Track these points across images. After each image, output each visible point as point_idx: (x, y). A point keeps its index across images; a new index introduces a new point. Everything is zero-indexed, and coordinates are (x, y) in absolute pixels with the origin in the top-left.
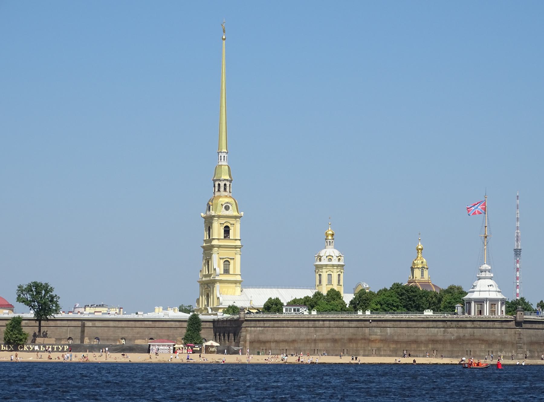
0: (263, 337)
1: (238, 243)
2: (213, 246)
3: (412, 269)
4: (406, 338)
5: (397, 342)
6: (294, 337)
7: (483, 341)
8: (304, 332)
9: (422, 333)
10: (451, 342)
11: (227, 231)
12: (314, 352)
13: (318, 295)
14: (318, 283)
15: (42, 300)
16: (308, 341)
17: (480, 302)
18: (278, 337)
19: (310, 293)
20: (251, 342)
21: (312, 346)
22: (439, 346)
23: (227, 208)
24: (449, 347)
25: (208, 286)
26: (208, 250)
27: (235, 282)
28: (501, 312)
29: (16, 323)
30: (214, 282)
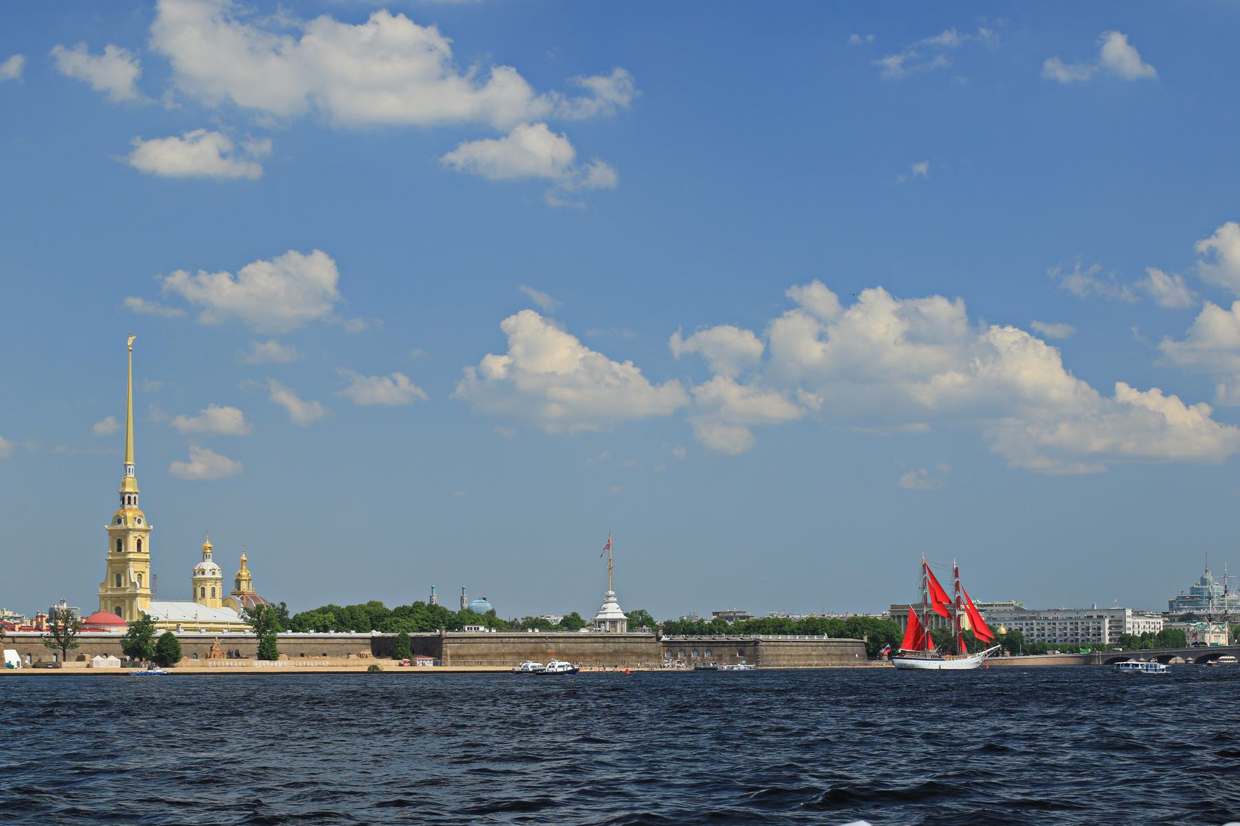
0: (460, 652)
1: (148, 557)
2: (130, 560)
3: (238, 582)
4: (575, 652)
5: (568, 655)
6: (486, 651)
7: (633, 653)
14: (199, 595)
17: (614, 622)
18: (472, 652)
20: (452, 656)
22: (601, 658)
23: (139, 522)
24: (608, 658)
27: (146, 596)
30: (137, 595)
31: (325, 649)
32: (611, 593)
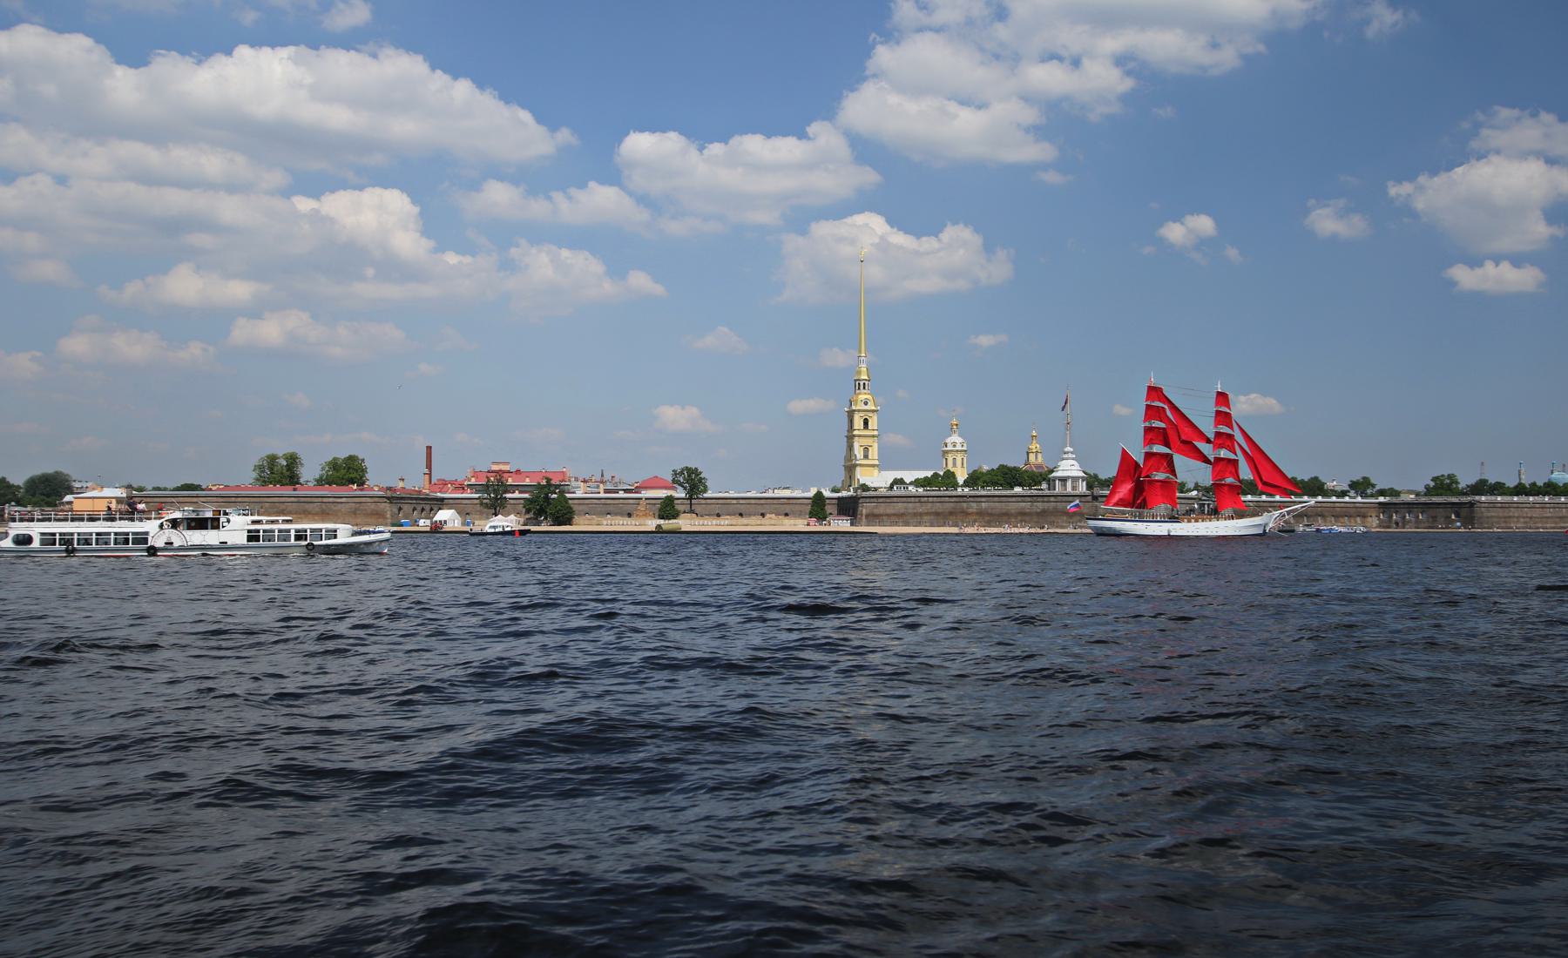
0: (876, 511)
8: (911, 507)
9: (1013, 507)
10: (1038, 514)
11: (866, 422)
12: (919, 524)
13: (936, 475)
15: (693, 482)
16: (915, 514)
17: (1064, 480)
19: (929, 474)
21: (918, 518)
25: (850, 469)
26: (850, 438)
28: (1082, 488)
29: (669, 501)
31: (787, 509)
32: (1068, 449)
